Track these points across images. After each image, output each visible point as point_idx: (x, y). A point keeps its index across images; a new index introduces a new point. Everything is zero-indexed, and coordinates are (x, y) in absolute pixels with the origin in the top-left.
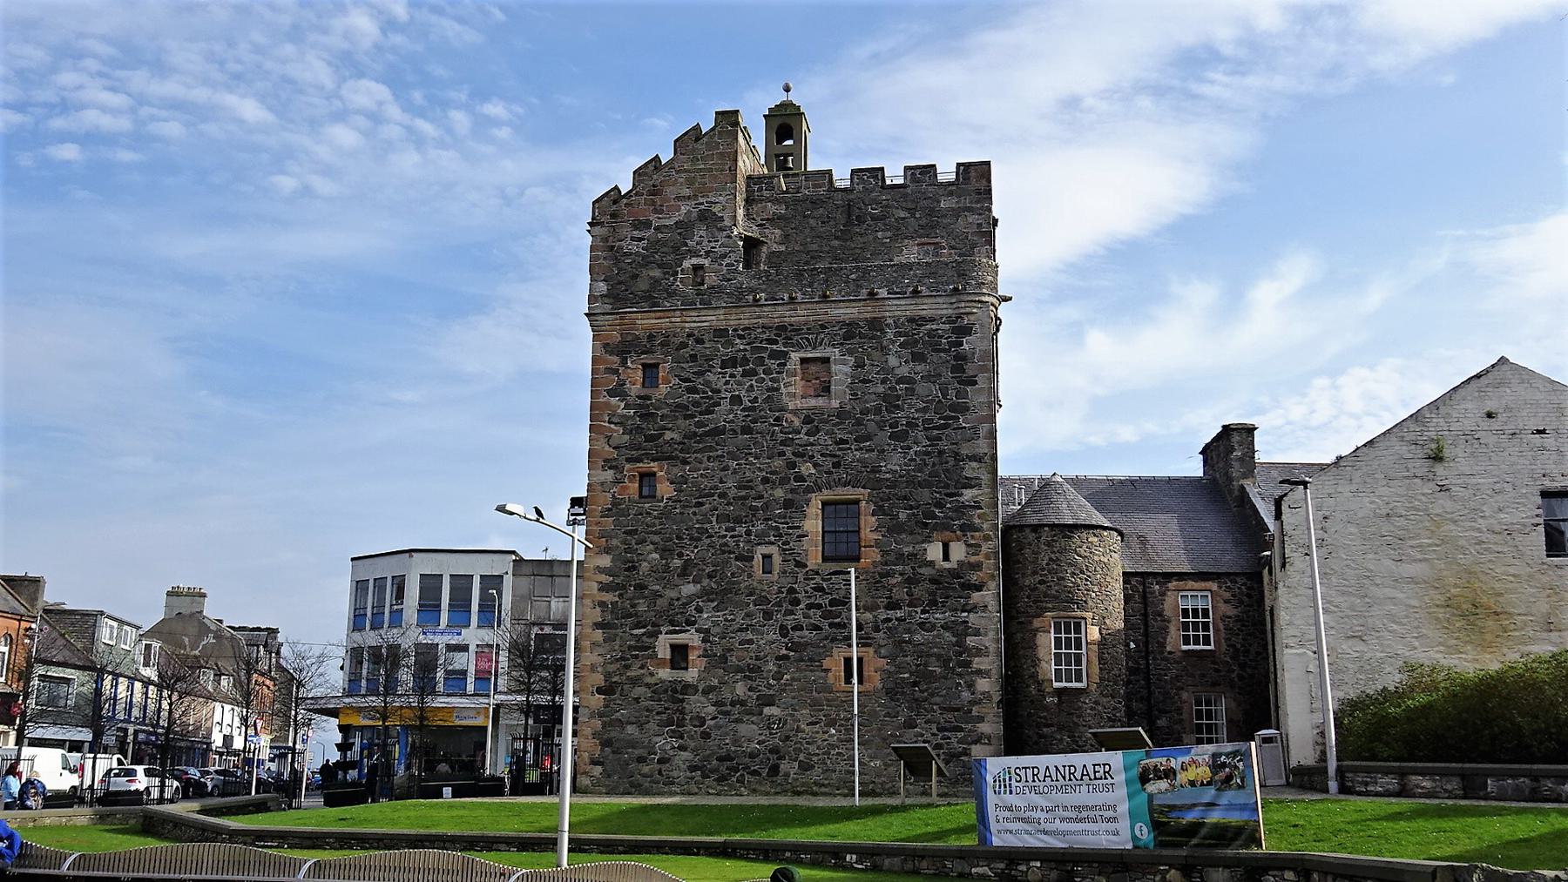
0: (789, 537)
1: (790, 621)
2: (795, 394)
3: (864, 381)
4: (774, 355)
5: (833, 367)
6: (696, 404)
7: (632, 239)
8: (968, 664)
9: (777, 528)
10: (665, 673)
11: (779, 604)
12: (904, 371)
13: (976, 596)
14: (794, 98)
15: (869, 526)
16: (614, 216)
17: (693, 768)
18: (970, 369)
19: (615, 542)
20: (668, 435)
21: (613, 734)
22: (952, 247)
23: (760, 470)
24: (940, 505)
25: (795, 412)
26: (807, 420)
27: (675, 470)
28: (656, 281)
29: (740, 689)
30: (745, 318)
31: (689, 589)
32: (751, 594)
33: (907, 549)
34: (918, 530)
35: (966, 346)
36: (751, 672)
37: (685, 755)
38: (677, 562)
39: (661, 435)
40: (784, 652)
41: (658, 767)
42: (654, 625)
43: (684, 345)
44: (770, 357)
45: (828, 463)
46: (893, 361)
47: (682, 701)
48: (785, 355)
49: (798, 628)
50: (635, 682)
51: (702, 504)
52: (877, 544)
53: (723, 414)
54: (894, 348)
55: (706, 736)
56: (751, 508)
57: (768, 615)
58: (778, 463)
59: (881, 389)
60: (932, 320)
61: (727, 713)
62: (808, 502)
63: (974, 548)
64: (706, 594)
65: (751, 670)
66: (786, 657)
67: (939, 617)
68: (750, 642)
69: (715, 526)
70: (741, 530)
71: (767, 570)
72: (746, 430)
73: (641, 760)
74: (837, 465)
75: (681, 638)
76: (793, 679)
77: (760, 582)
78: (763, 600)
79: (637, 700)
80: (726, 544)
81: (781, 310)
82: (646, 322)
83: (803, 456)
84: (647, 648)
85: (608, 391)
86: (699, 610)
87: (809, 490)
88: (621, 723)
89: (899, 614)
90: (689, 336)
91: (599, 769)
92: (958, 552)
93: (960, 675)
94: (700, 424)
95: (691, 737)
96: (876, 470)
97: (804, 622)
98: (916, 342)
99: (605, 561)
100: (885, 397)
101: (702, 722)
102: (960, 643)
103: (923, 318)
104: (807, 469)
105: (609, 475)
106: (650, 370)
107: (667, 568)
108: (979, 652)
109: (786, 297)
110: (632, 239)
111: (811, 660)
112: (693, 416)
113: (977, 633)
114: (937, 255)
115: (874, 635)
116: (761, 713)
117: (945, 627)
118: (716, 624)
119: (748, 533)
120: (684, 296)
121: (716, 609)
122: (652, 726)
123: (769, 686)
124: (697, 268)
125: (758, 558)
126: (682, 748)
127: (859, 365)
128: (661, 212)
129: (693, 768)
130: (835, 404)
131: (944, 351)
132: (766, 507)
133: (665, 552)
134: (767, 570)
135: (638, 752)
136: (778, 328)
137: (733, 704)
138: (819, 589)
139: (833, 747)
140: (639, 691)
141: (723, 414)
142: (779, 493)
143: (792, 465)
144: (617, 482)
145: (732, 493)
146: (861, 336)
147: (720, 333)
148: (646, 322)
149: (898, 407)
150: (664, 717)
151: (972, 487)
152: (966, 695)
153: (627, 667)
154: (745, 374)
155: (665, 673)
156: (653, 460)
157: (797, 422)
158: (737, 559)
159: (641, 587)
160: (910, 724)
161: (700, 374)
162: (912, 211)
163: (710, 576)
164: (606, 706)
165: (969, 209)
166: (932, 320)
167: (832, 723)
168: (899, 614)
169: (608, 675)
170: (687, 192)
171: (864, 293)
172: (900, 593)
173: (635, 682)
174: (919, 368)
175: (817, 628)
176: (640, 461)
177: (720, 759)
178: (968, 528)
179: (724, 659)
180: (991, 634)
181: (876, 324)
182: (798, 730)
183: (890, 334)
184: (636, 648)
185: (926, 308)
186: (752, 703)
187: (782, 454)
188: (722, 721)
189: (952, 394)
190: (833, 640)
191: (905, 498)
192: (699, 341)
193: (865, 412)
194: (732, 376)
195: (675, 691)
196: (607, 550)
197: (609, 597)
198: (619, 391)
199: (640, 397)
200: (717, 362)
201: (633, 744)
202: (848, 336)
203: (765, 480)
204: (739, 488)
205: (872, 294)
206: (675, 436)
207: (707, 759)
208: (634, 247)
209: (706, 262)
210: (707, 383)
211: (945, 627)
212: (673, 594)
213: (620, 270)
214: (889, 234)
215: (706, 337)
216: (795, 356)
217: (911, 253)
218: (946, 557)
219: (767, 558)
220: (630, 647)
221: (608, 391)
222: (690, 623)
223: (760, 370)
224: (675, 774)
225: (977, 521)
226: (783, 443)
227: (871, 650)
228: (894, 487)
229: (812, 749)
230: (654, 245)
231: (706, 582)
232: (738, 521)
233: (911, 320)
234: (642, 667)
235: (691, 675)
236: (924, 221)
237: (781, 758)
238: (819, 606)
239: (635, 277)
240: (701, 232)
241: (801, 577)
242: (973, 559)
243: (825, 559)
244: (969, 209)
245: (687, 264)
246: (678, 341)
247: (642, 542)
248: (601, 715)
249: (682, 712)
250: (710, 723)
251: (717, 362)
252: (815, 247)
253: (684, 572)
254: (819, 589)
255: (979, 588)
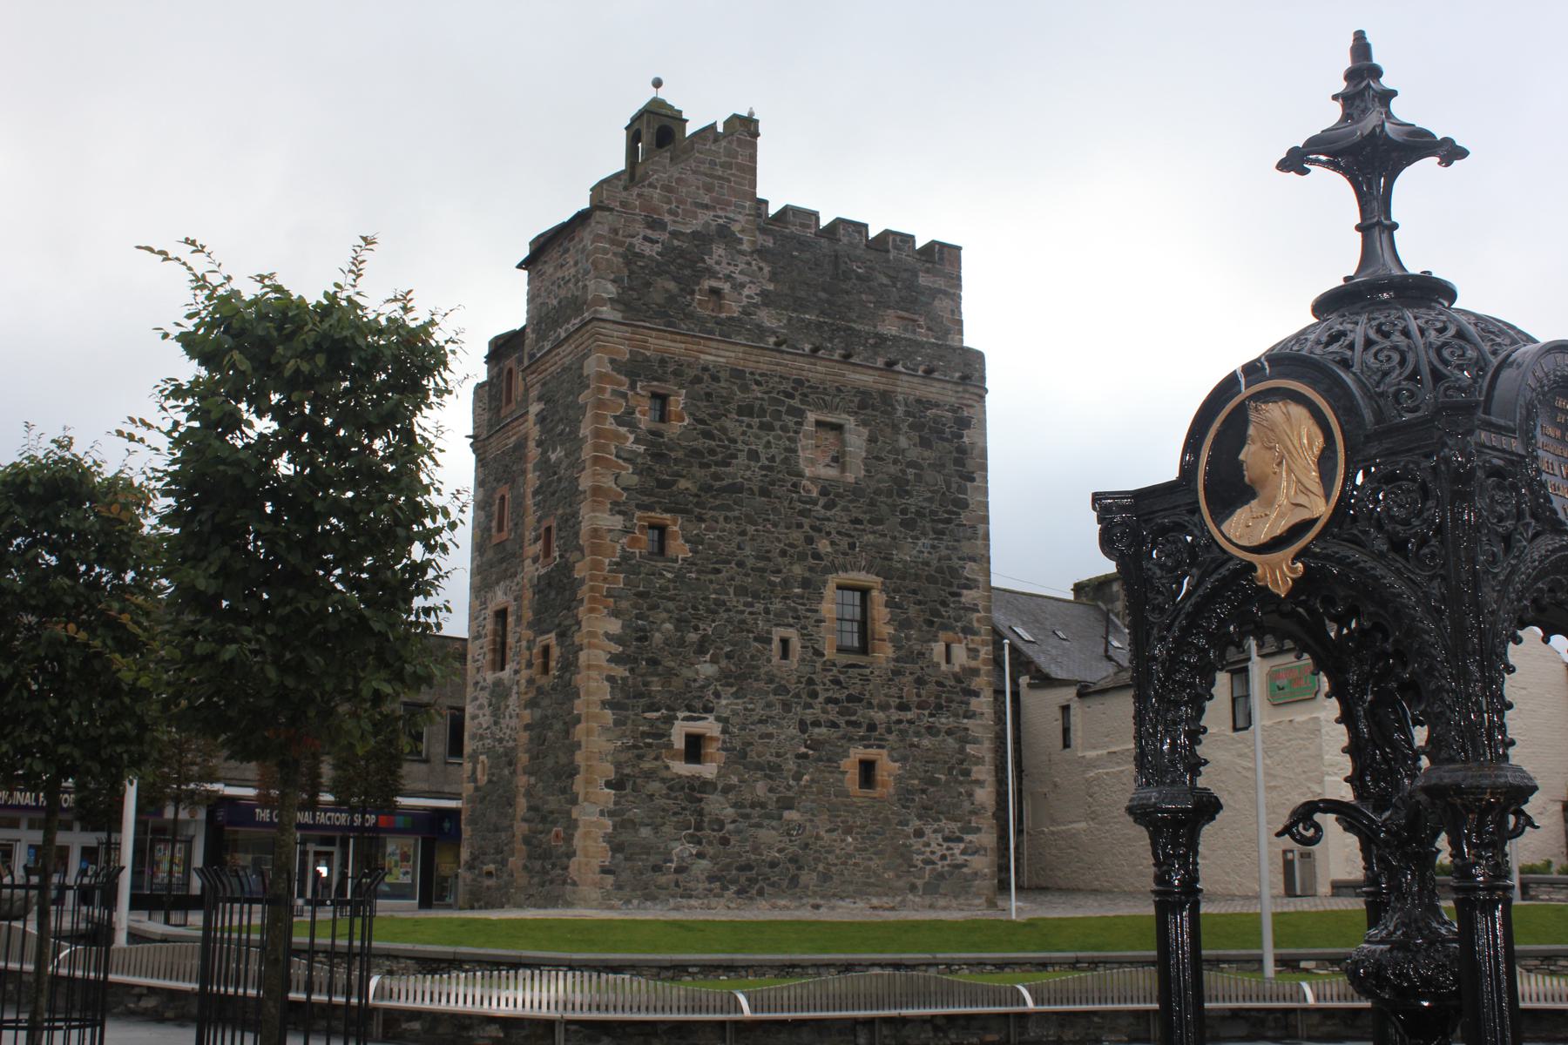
0: (805, 619)
1: (809, 715)
2: (814, 465)
3: (878, 458)
4: (793, 411)
5: (847, 436)
6: (712, 452)
7: (646, 238)
8: (967, 773)
9: (795, 610)
10: (681, 768)
11: (798, 695)
12: (914, 453)
13: (974, 703)
14: (662, 94)
15: (880, 613)
16: (624, 204)
17: (711, 879)
18: (970, 464)
19: (624, 604)
20: (683, 484)
21: (625, 837)
22: (929, 329)
23: (779, 541)
24: (944, 604)
25: (814, 480)
26: (824, 492)
27: (690, 526)
28: (671, 299)
29: (761, 788)
30: (764, 363)
31: (706, 669)
32: (771, 681)
33: (917, 647)
34: (925, 628)
35: (965, 439)
36: (772, 771)
37: (704, 863)
38: (693, 637)
39: (675, 482)
40: (803, 750)
41: (672, 877)
42: (669, 708)
43: (697, 380)
44: (788, 412)
45: (844, 543)
46: (903, 442)
47: (700, 800)
48: (799, 413)
49: (816, 724)
50: (649, 775)
51: (718, 571)
52: (893, 639)
53: (741, 470)
54: (904, 427)
55: (725, 842)
56: (771, 583)
57: (787, 707)
58: (796, 536)
59: (893, 469)
60: (937, 405)
61: (747, 817)
62: (825, 583)
63: (973, 653)
64: (725, 677)
65: (771, 769)
66: (805, 756)
67: (944, 721)
68: (770, 736)
69: (732, 599)
70: (759, 607)
71: (785, 654)
72: (764, 492)
73: (656, 868)
74: (852, 546)
75: (697, 727)
76: (812, 780)
77: (779, 667)
78: (781, 690)
79: (651, 797)
80: (743, 622)
81: (801, 363)
82: (658, 343)
83: (820, 531)
84: (662, 736)
85: (615, 418)
86: (717, 695)
87: (826, 571)
88: (633, 824)
89: (909, 715)
90: (705, 369)
91: (610, 879)
92: (960, 654)
93: (961, 783)
94: (716, 477)
95: (710, 843)
96: (888, 558)
97: (823, 718)
98: (923, 425)
99: (615, 626)
100: (895, 479)
101: (722, 826)
102: (962, 750)
103: (929, 402)
104: (824, 546)
105: (618, 522)
106: (661, 399)
107: (682, 643)
108: (979, 761)
109: (807, 347)
110: (646, 238)
111: (829, 760)
112: (709, 466)
113: (975, 741)
114: (914, 332)
115: (887, 736)
116: (780, 817)
117: (949, 733)
118: (735, 713)
119: (767, 611)
120: (701, 321)
121: (736, 695)
122: (667, 829)
123: (789, 788)
124: (715, 292)
125: (776, 645)
126: (700, 855)
127: (872, 440)
128: (676, 214)
129: (711, 879)
130: (850, 477)
131: (946, 440)
132: (786, 583)
133: (681, 623)
134: (785, 654)
135: (654, 859)
136: (795, 381)
137: (753, 806)
138: (836, 682)
139: (850, 856)
140: (654, 786)
141: (741, 470)
142: (797, 569)
143: (809, 540)
144: (626, 531)
145: (750, 562)
146: (874, 408)
147: (737, 374)
148: (658, 343)
149: (908, 493)
150: (681, 818)
151: (970, 588)
152: (967, 804)
153: (640, 757)
154: (762, 426)
155: (681, 768)
156: (666, 511)
157: (815, 494)
158: (756, 639)
159: (653, 662)
160: (919, 833)
161: (716, 417)
162: (894, 280)
163: (729, 656)
164: (616, 803)
165: (946, 293)
166: (937, 405)
167: (848, 831)
168: (909, 715)
169: (618, 766)
170: (706, 200)
171: (880, 362)
172: (910, 693)
173: (649, 775)
174: (927, 454)
175: (834, 725)
176: (653, 510)
177: (741, 869)
178: (969, 630)
179: (744, 755)
180: (987, 744)
181: (886, 397)
182: (818, 837)
183: (900, 410)
184: (648, 735)
185: (932, 391)
186: (772, 806)
187: (800, 526)
188: (743, 825)
189: (954, 486)
190: (851, 739)
191: (914, 592)
192: (715, 379)
193: (878, 492)
194: (749, 426)
195: (692, 788)
196: (616, 613)
197: (620, 671)
198: (626, 419)
199: (652, 433)
200: (733, 406)
201: (647, 849)
202: (863, 406)
203: (783, 553)
204: (757, 558)
205: (890, 364)
206: (688, 484)
207: (728, 867)
208: (649, 250)
209: (726, 287)
210: (723, 430)
211: (949, 733)
212: (687, 673)
213: (631, 272)
214: (872, 298)
215: (722, 375)
216: (811, 417)
217: (890, 328)
218: (948, 660)
219: (785, 642)
220: (644, 734)
221: (615, 418)
222: (708, 709)
223: (777, 424)
224: (691, 885)
225: (975, 624)
226: (802, 513)
227: (884, 752)
228: (904, 579)
229: (831, 858)
230: (667, 250)
231: (724, 663)
232: (756, 596)
233: (919, 401)
234: (656, 759)
235: (708, 770)
236: (904, 293)
237: (800, 868)
238: (835, 701)
239: (648, 284)
240: (719, 250)
241: (819, 666)
242: (973, 664)
243: (841, 650)
244: (946, 293)
245: (707, 284)
246: (692, 373)
247: (654, 607)
248: (611, 814)
249: (701, 813)
250: (730, 827)
251: (733, 406)
252: (802, 294)
253: (701, 649)
254: (836, 682)
255: (976, 694)
